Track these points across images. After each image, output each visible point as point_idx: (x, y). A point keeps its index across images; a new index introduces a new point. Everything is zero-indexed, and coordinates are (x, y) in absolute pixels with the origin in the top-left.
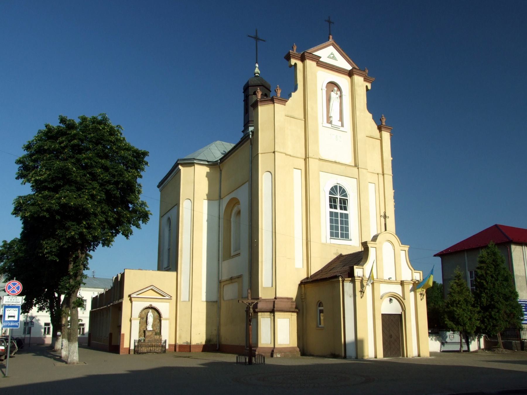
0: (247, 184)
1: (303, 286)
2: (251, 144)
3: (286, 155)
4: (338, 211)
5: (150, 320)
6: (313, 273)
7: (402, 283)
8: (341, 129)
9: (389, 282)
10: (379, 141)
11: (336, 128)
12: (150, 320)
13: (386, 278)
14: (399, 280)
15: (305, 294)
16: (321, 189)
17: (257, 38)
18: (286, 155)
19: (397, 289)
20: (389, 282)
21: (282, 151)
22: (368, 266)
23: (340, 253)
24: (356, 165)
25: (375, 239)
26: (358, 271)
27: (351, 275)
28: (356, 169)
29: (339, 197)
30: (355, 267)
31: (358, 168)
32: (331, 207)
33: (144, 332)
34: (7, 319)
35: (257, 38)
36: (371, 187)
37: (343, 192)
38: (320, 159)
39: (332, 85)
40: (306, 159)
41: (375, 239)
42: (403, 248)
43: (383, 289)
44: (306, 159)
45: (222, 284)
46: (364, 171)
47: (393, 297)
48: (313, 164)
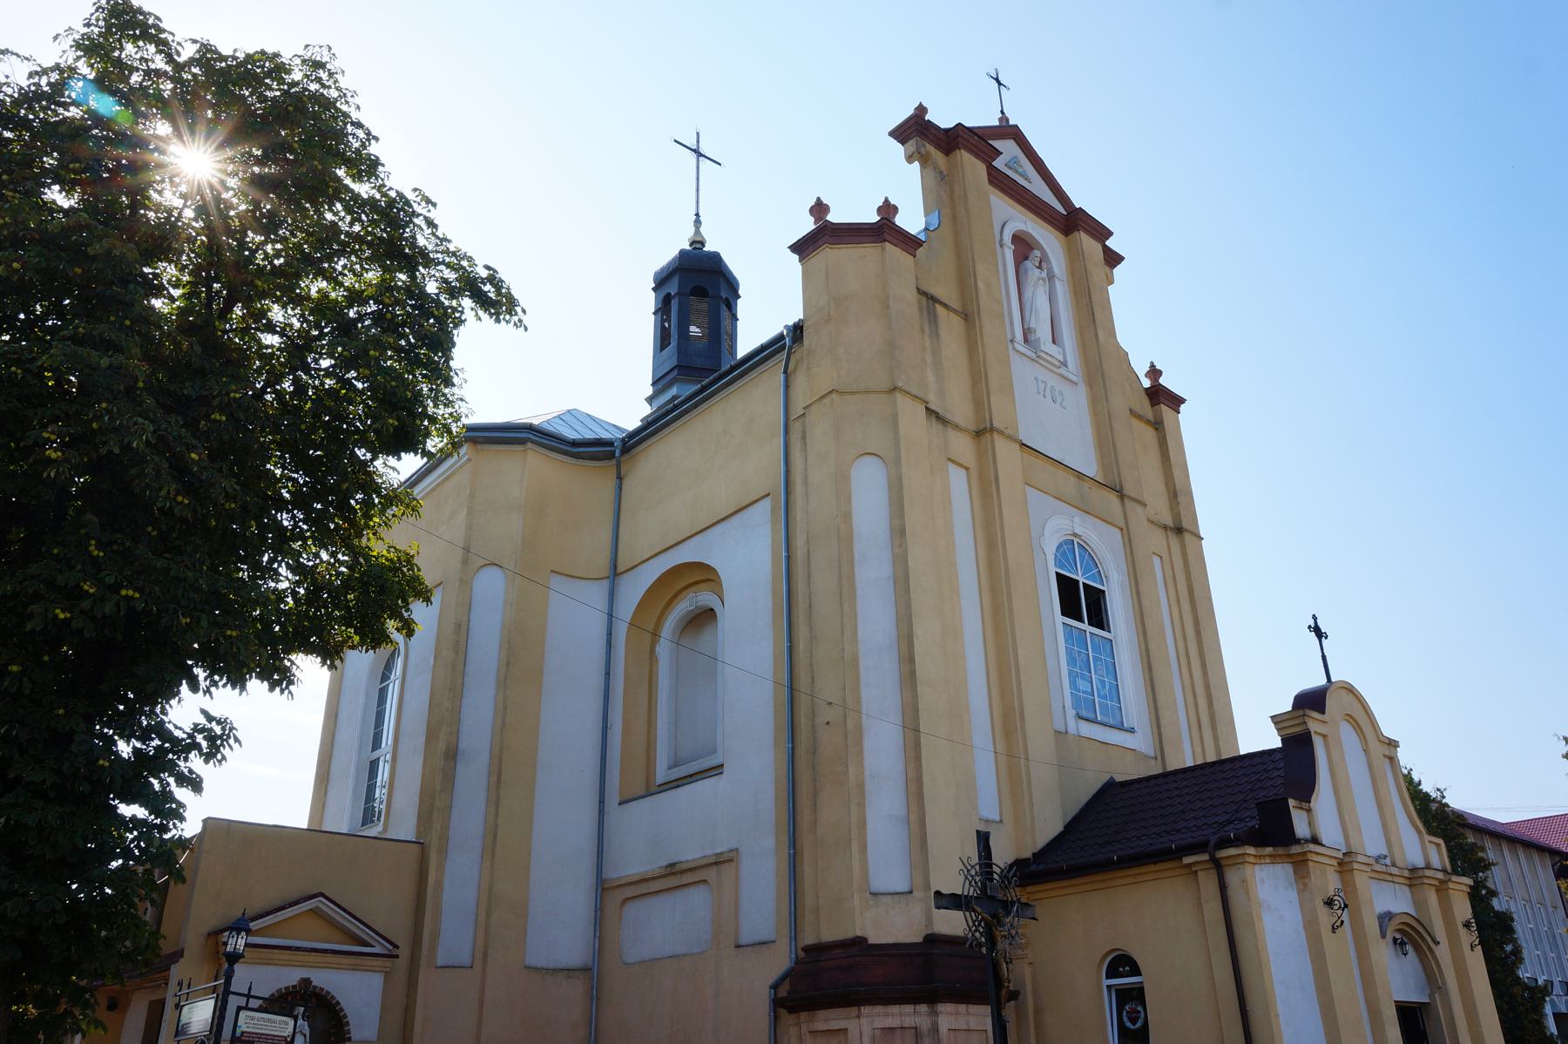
2: (785, 372)
8: (1063, 371)
10: (1150, 433)
23: (1106, 778)
27: (1275, 834)
28: (1113, 498)
29: (1082, 580)
30: (1292, 802)
37: (1092, 562)
45: (615, 898)
46: (1139, 509)
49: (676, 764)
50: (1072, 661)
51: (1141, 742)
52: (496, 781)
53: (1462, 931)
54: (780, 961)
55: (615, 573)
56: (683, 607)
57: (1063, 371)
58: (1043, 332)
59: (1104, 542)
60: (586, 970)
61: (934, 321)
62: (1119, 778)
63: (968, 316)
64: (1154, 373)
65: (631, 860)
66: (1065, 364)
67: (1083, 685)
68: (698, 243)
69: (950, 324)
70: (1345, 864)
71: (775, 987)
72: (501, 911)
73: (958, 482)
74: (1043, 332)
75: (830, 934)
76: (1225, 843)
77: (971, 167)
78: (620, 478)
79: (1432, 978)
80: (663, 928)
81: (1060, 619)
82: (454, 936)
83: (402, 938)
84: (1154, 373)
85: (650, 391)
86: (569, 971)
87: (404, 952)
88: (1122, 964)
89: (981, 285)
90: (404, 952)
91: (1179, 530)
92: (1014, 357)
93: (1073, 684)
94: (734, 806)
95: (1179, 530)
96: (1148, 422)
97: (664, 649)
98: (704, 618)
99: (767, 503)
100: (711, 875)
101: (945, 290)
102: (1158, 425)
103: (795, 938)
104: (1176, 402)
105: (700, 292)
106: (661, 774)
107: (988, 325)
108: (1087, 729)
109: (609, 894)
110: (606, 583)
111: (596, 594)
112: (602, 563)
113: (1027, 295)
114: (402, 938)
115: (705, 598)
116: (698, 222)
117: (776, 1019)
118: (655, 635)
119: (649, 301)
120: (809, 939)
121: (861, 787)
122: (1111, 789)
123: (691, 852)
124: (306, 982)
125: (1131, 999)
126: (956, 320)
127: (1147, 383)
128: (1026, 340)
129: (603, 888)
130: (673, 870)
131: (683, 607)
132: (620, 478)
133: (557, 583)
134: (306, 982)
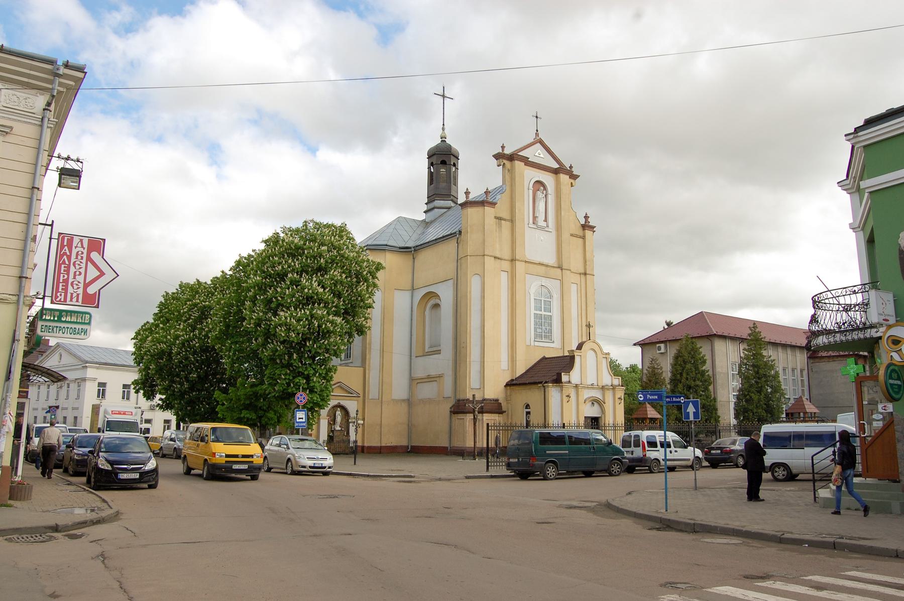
0: (451, 282)
4: (543, 313)
6: (518, 375)
12: (339, 419)
13: (589, 383)
19: (598, 394)
25: (580, 347)
26: (564, 378)
27: (558, 381)
28: (559, 270)
29: (543, 299)
33: (331, 431)
36: (574, 288)
38: (526, 262)
39: (539, 183)
41: (580, 347)
43: (586, 394)
46: (568, 272)
47: (595, 401)
50: (536, 324)
51: (557, 344)
52: (382, 351)
53: (617, 401)
55: (413, 289)
56: (432, 302)
58: (541, 217)
61: (500, 226)
63: (512, 221)
64: (586, 217)
65: (419, 374)
66: (548, 226)
67: (538, 330)
68: (443, 138)
69: (506, 225)
70: (576, 386)
73: (504, 277)
74: (541, 217)
75: (462, 397)
76: (546, 382)
77: (518, 164)
79: (603, 411)
80: (427, 391)
81: (533, 311)
82: (373, 392)
84: (586, 217)
86: (403, 400)
88: (528, 406)
90: (361, 395)
91: (585, 274)
92: (527, 229)
94: (441, 363)
95: (585, 274)
96: (580, 237)
97: (427, 312)
98: (437, 306)
99: (451, 282)
100: (437, 379)
101: (505, 214)
102: (584, 237)
104: (592, 228)
105: (444, 163)
107: (518, 223)
108: (536, 344)
109: (413, 381)
111: (408, 295)
112: (409, 286)
113: (536, 205)
115: (438, 301)
116: (443, 129)
119: (425, 163)
120: (458, 397)
122: (544, 358)
123: (433, 373)
125: (528, 413)
126: (508, 224)
130: (429, 377)
131: (432, 302)
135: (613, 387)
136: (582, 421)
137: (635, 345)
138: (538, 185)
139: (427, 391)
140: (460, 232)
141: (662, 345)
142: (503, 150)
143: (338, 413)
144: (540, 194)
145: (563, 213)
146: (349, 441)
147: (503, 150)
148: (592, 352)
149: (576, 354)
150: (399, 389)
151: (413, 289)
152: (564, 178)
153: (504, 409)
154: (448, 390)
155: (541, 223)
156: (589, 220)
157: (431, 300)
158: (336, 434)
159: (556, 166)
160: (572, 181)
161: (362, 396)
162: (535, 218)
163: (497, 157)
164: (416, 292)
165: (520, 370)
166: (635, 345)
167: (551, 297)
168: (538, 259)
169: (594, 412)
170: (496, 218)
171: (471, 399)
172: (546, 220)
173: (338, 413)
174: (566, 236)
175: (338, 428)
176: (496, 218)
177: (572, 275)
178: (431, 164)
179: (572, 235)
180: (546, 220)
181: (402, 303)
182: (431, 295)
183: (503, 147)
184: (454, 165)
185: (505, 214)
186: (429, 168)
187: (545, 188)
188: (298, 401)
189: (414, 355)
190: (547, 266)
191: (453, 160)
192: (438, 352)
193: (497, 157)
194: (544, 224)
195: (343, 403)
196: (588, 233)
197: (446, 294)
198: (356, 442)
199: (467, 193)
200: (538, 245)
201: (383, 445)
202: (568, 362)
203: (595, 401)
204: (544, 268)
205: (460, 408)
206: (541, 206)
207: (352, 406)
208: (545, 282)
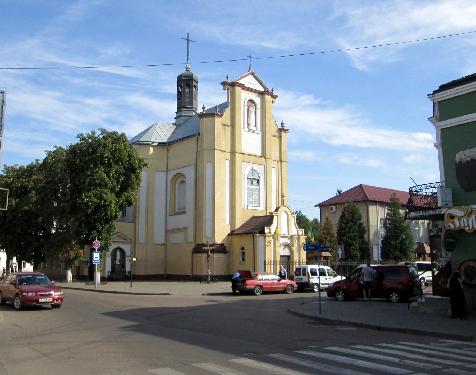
0: (193, 167)
1: (230, 236)
2: (197, 141)
3: (222, 151)
5: (118, 256)
7: (291, 238)
9: (284, 236)
11: (252, 131)
12: (118, 256)
14: (290, 235)
15: (232, 241)
16: (243, 173)
17: (188, 40)
18: (222, 151)
20: (284, 236)
21: (219, 149)
22: (273, 227)
24: (264, 155)
26: (267, 230)
27: (262, 232)
28: (264, 159)
30: (266, 227)
31: (266, 159)
32: (248, 184)
33: (113, 265)
34: (94, 259)
35: (188, 40)
36: (274, 170)
38: (242, 154)
39: (251, 101)
40: (233, 153)
41: (277, 210)
42: (293, 216)
44: (233, 153)
46: (270, 160)
47: (286, 245)
48: (238, 157)
49: (179, 209)
50: (248, 194)
51: (262, 208)
54: (193, 246)
56: (179, 180)
57: (256, 132)
58: (252, 123)
59: (260, 169)
60: (164, 244)
61: (225, 130)
62: (256, 215)
64: (282, 124)
65: (171, 227)
71: (193, 250)
72: (149, 234)
73: (227, 163)
74: (252, 123)
75: (200, 243)
77: (237, 89)
78: (168, 150)
79: (291, 252)
80: (177, 238)
82: (141, 238)
83: (132, 238)
84: (282, 124)
85: (176, 111)
86: (161, 244)
87: (133, 241)
88: (243, 249)
89: (236, 120)
90: (133, 241)
92: (243, 132)
93: (248, 198)
94: (186, 220)
98: (183, 182)
102: (280, 137)
103: (196, 242)
104: (286, 131)
105: (188, 85)
106: (177, 211)
109: (168, 232)
110: (165, 173)
111: (164, 174)
114: (132, 238)
115: (184, 179)
117: (193, 255)
118: (175, 185)
120: (197, 243)
121: (205, 220)
122: (254, 217)
123: (181, 226)
124: (119, 247)
125: (244, 253)
127: (280, 126)
128: (248, 128)
129: (167, 230)
131: (179, 180)
132: (168, 150)
133: (156, 172)
134: (119, 247)
135: (299, 237)
136: (278, 259)
137: (316, 206)
138: (250, 103)
139: (177, 238)
140: (199, 134)
141: (334, 207)
142: (227, 79)
143: (118, 253)
144: (251, 108)
145: (266, 121)
146: (125, 271)
147: (227, 79)
148: (285, 213)
149: (274, 214)
150: (159, 238)
151: (167, 171)
152: (268, 98)
153: (227, 250)
154: (191, 238)
155: (252, 127)
156: (284, 125)
157: (179, 178)
158: (116, 267)
159: (262, 89)
160: (273, 99)
161: (133, 242)
162: (248, 124)
163: (224, 84)
164: (169, 173)
165: (238, 225)
166: (316, 206)
167: (259, 176)
168: (249, 152)
169: (286, 252)
170: (223, 125)
171: (206, 244)
172: (255, 126)
173: (118, 253)
174: (268, 136)
175: (118, 263)
176: (223, 125)
177: (273, 162)
178: (179, 86)
179: (273, 136)
180: (255, 126)
181: (160, 180)
182: (179, 175)
183: (227, 78)
184: (195, 87)
185: (228, 123)
186: (178, 89)
187: (255, 105)
188: (94, 246)
189: (168, 215)
190: (255, 156)
191: (194, 83)
192: (184, 213)
193: (224, 84)
194: (254, 128)
195: (122, 246)
196: (283, 134)
197: (189, 174)
198: (129, 272)
199: (203, 108)
200: (250, 142)
201: (148, 274)
202: (269, 220)
203: (286, 245)
204: (254, 157)
205: (198, 249)
206: (252, 116)
207: (127, 248)
208: (255, 167)
